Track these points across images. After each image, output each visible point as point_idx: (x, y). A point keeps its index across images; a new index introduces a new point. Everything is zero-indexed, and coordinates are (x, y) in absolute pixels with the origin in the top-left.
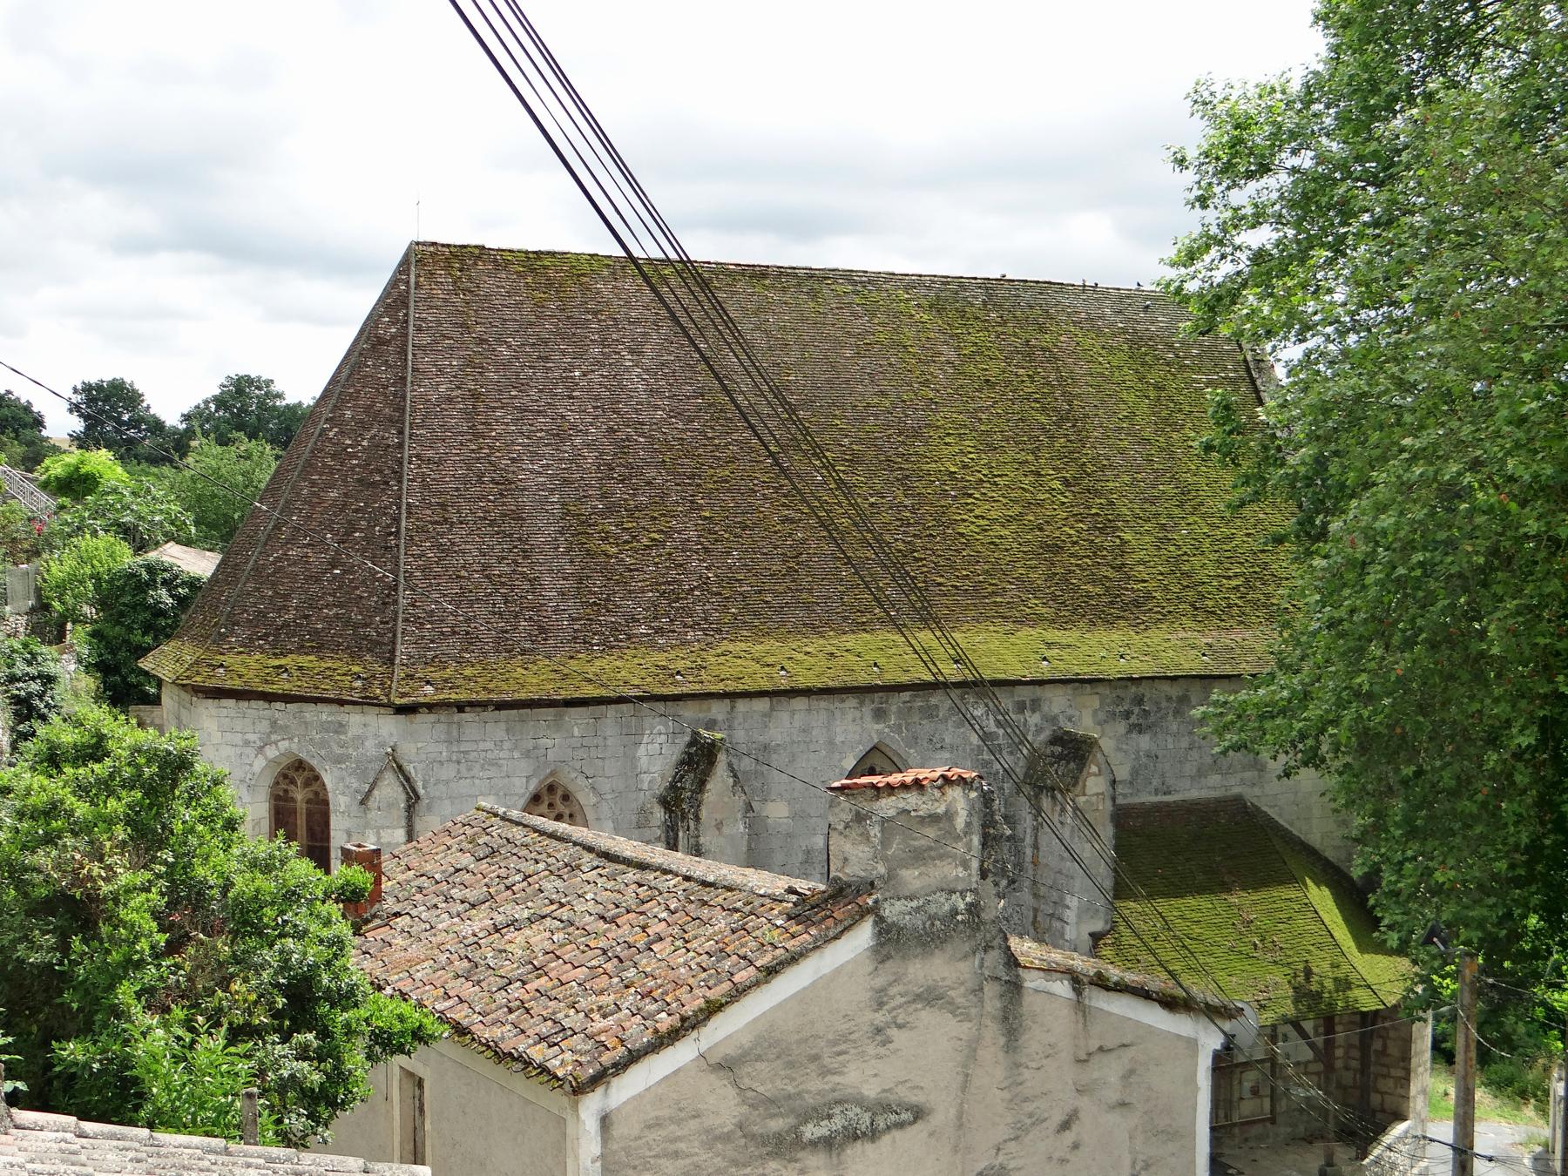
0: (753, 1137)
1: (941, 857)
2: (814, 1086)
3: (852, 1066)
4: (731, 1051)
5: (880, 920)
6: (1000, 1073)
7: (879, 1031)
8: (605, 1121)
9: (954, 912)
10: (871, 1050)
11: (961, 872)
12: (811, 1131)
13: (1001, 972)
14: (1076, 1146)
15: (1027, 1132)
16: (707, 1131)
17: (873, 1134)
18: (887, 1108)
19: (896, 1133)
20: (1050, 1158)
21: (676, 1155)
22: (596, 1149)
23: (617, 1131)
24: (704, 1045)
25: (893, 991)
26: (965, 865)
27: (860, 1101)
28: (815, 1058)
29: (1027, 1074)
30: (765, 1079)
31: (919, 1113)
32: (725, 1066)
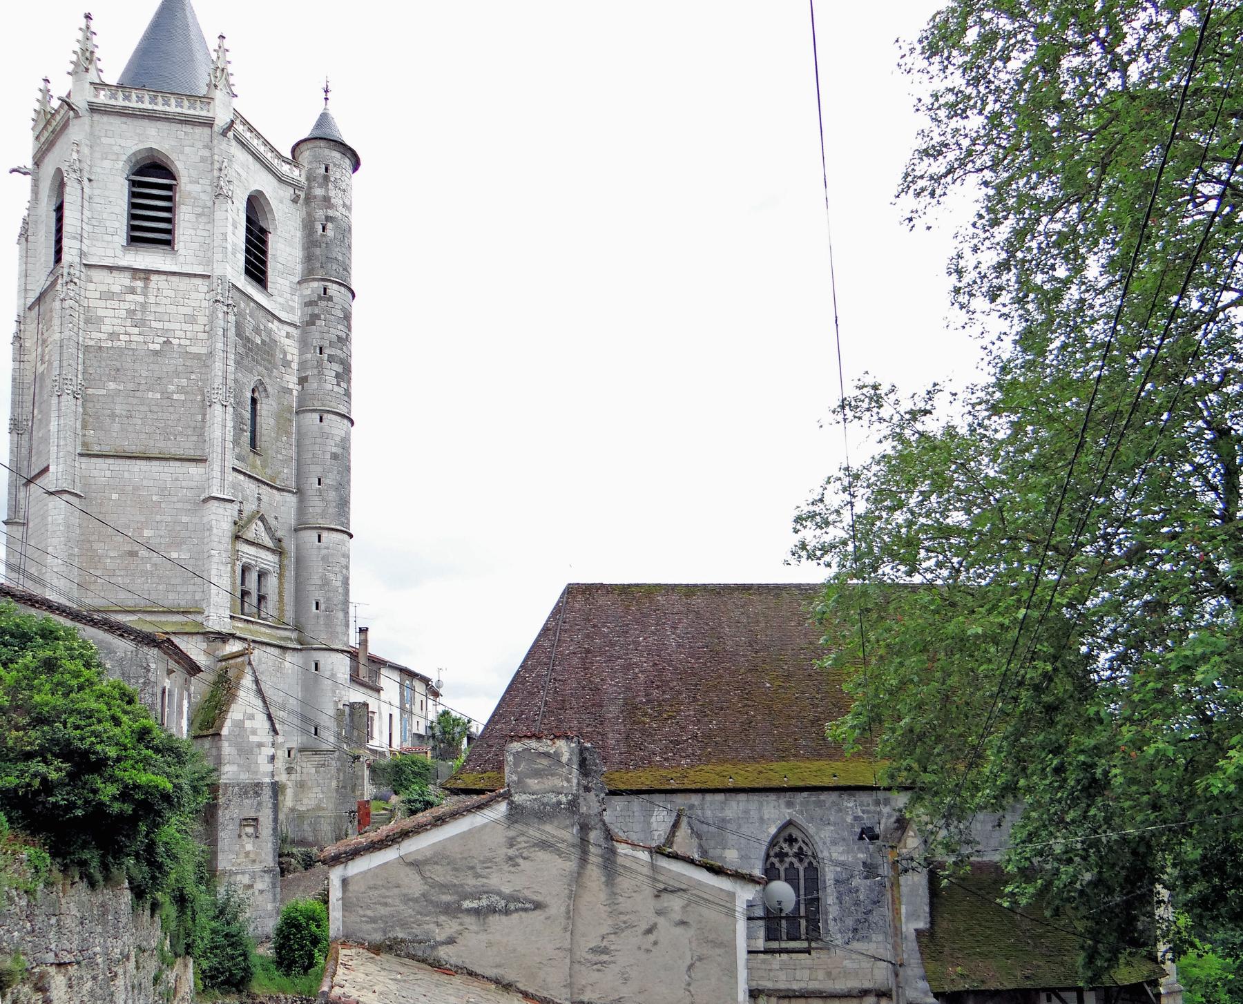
0: (432, 902)
1: (552, 775)
2: (471, 882)
3: (494, 875)
4: (419, 857)
5: (511, 803)
6: (603, 896)
7: (510, 859)
8: (345, 882)
9: (559, 803)
10: (506, 868)
11: (565, 784)
12: (467, 904)
13: (602, 842)
14: (655, 943)
15: (623, 931)
16: (405, 895)
17: (507, 912)
18: (517, 900)
19: (523, 914)
20: (639, 948)
21: (386, 904)
22: (340, 895)
23: (351, 888)
24: (402, 852)
25: (519, 839)
26: (568, 780)
27: (499, 894)
28: (472, 868)
29: (621, 899)
30: (440, 874)
31: (538, 906)
32: (416, 864)
